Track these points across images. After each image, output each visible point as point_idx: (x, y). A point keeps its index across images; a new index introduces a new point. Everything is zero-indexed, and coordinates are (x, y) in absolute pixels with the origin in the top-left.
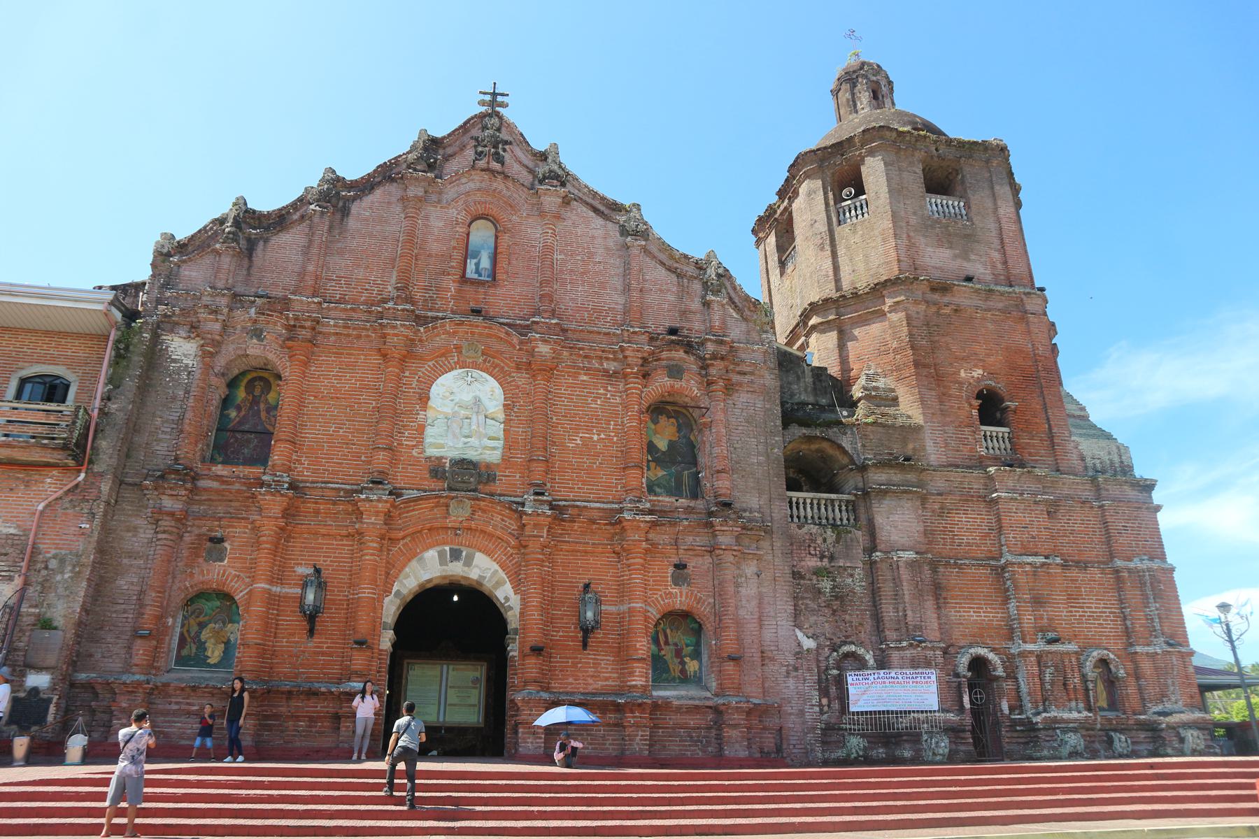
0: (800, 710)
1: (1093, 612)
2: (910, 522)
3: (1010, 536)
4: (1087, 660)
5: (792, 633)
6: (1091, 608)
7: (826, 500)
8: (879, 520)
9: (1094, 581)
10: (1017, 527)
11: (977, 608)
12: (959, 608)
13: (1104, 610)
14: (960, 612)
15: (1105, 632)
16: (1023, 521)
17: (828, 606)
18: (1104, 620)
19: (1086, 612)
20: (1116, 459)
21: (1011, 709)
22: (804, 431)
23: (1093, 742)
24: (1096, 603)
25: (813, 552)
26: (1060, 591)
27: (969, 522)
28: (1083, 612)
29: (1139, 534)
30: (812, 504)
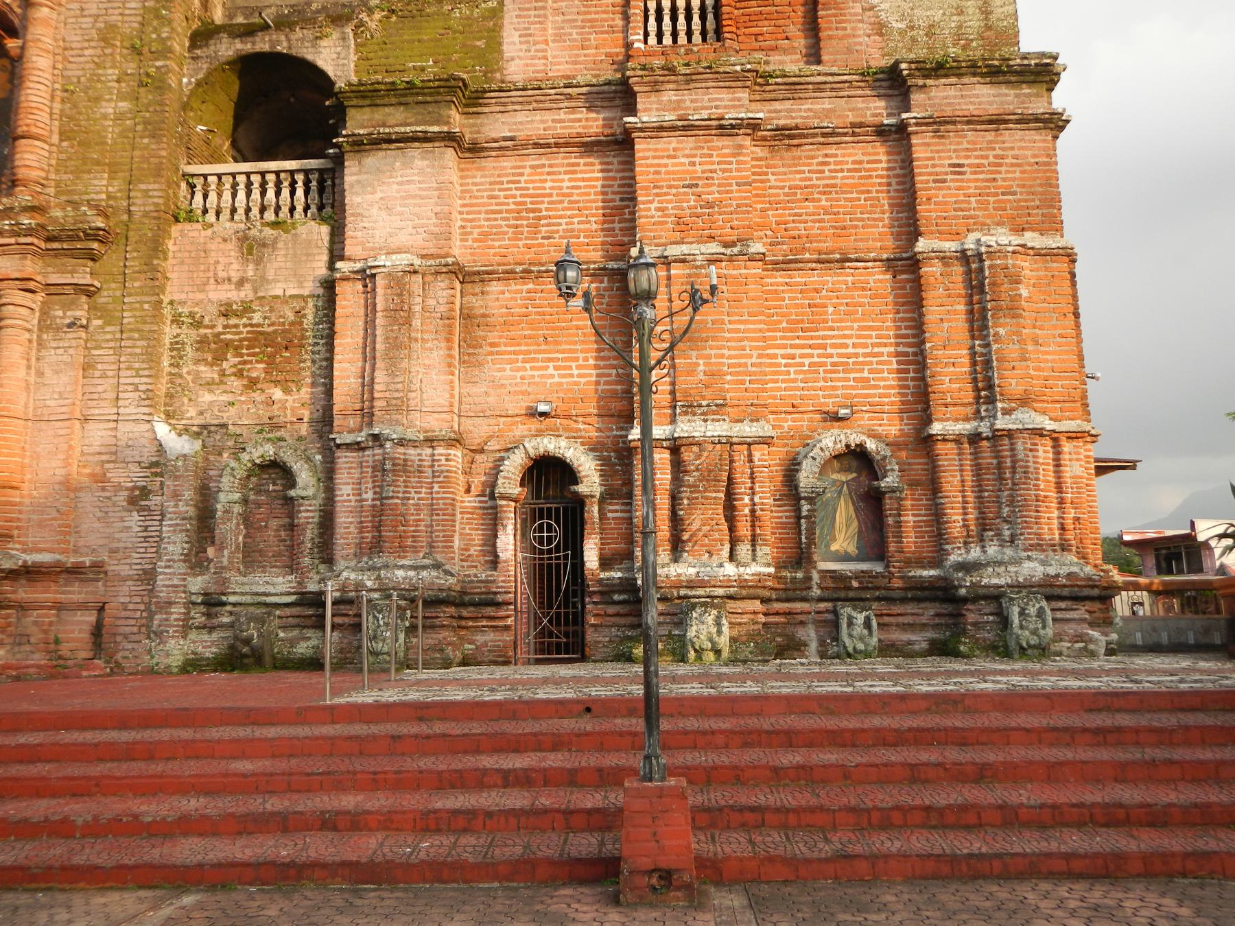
0: (145, 571)
1: (848, 356)
2: (422, 198)
3: (649, 209)
4: (806, 457)
5: (148, 426)
6: (846, 346)
7: (277, 173)
8: (354, 199)
9: (864, 289)
10: (670, 187)
11: (564, 359)
12: (524, 361)
13: (876, 350)
14: (525, 369)
15: (874, 396)
16: (687, 172)
17: (239, 374)
18: (870, 371)
19: (831, 356)
20: (974, 22)
21: (605, 563)
22: (239, 46)
23: (802, 623)
24: (859, 337)
25: (222, 274)
26: (750, 314)
27: (579, 188)
28: (819, 356)
29: (994, 179)
30: (249, 185)
